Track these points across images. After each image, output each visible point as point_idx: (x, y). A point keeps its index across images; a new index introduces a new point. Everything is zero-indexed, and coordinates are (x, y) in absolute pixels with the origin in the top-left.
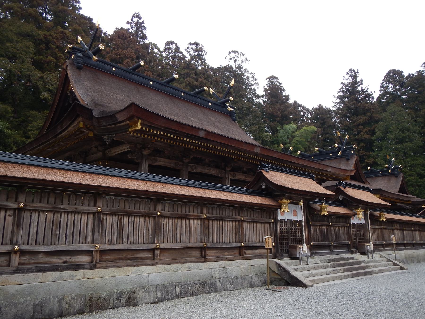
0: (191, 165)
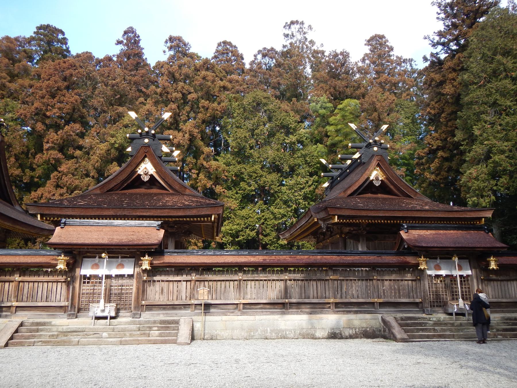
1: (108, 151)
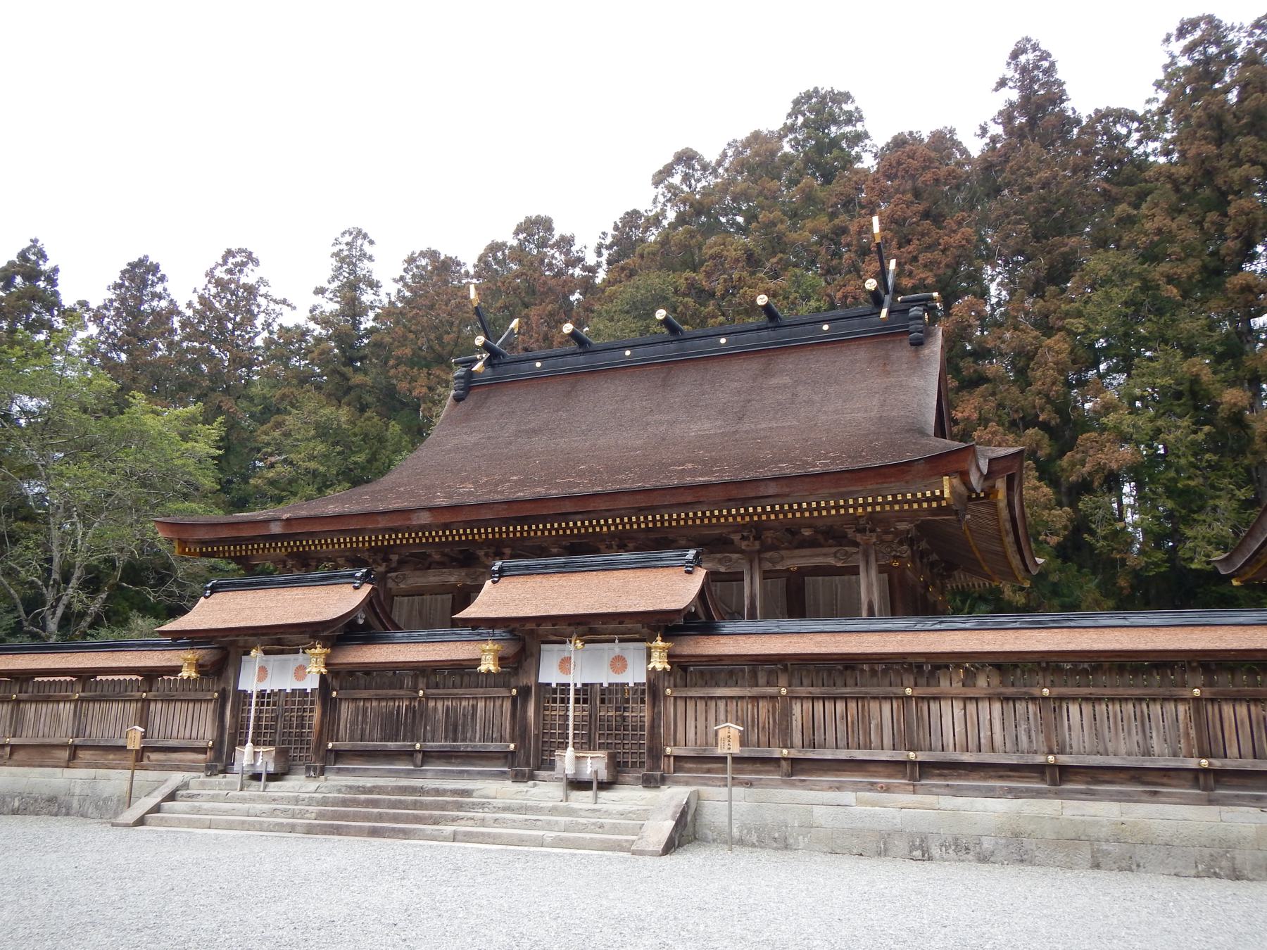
0: (393, 574)
1: (1072, 352)
